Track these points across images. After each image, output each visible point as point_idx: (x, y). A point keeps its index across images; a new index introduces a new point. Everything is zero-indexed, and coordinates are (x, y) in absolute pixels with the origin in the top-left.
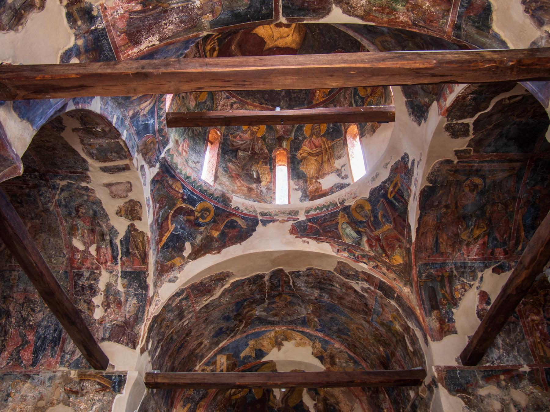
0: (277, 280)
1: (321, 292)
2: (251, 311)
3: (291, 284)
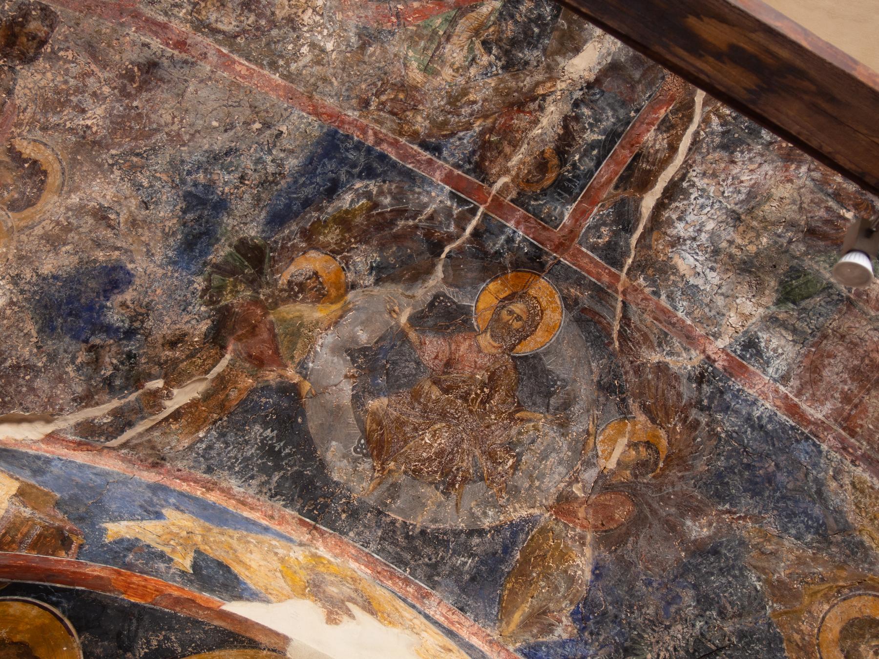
0: (609, 120)
1: (771, 321)
2: (321, 297)
3: (649, 202)
